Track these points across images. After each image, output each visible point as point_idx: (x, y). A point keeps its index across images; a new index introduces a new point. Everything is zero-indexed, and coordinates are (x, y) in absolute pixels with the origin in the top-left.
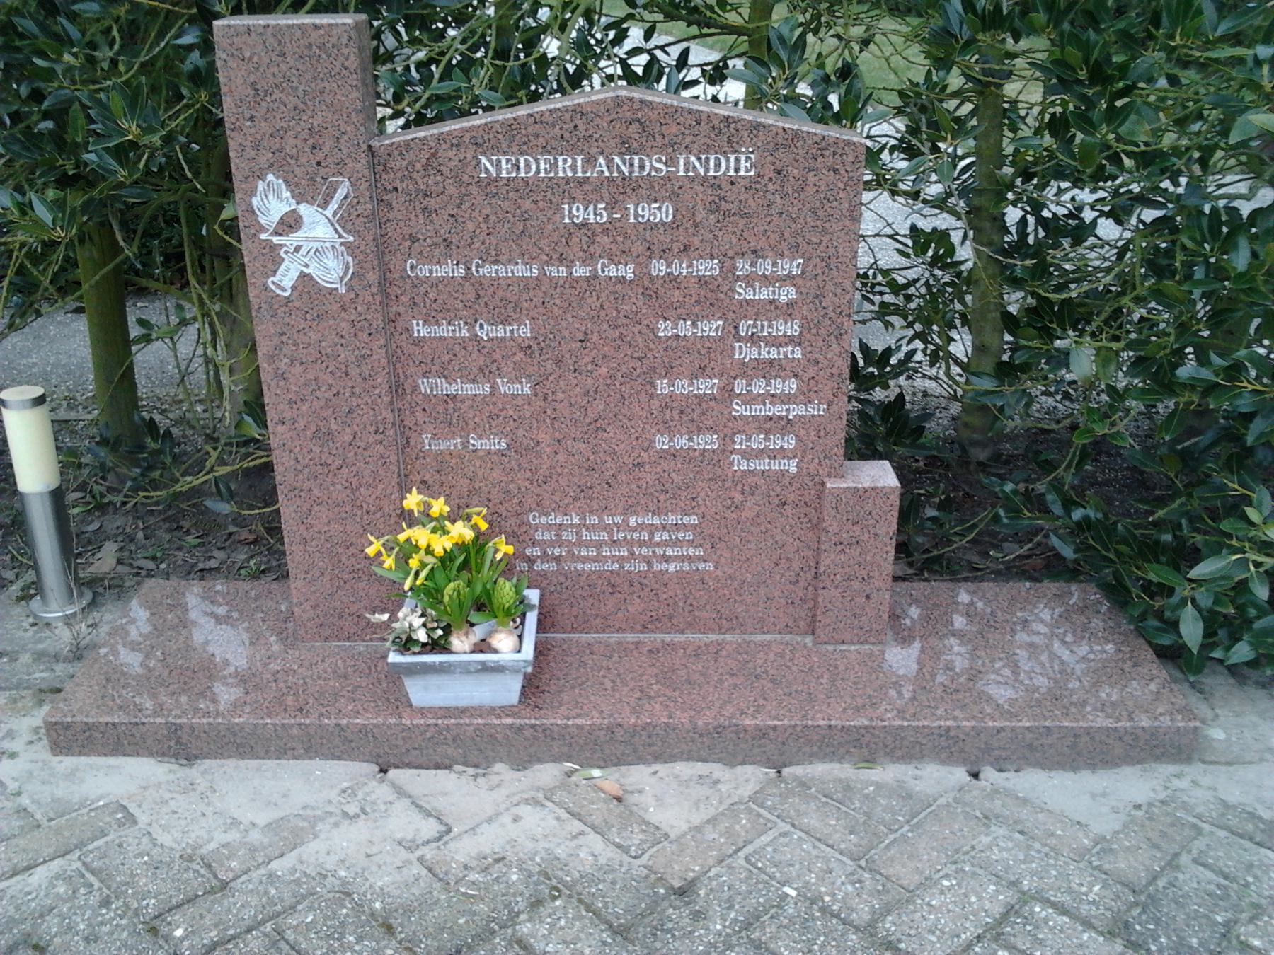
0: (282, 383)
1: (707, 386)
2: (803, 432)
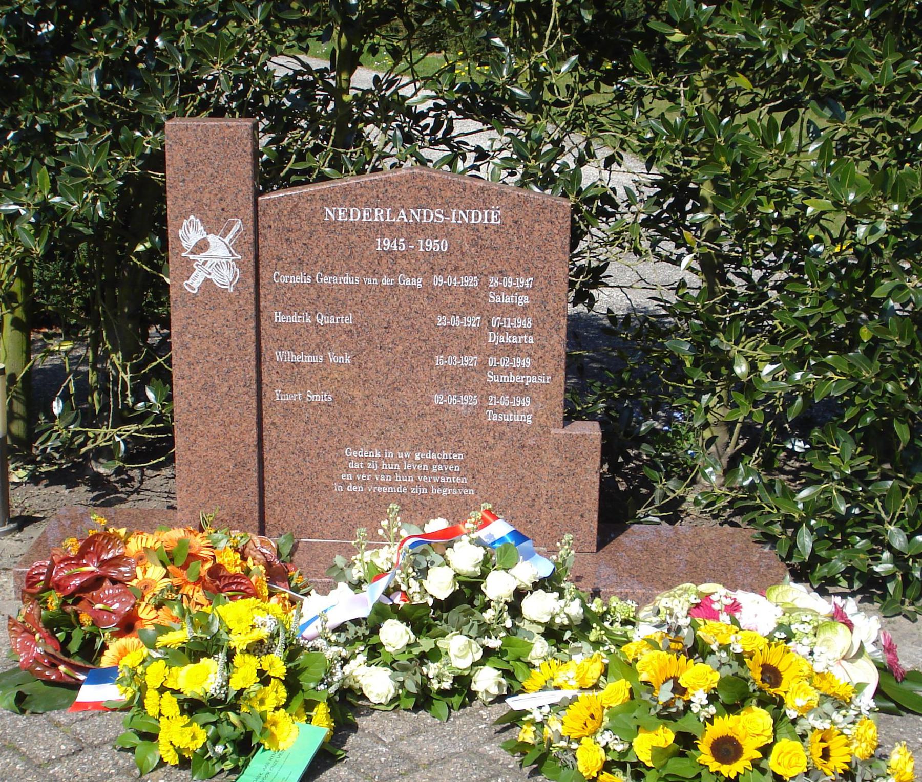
0: (185, 351)
1: (469, 361)
2: (535, 395)
